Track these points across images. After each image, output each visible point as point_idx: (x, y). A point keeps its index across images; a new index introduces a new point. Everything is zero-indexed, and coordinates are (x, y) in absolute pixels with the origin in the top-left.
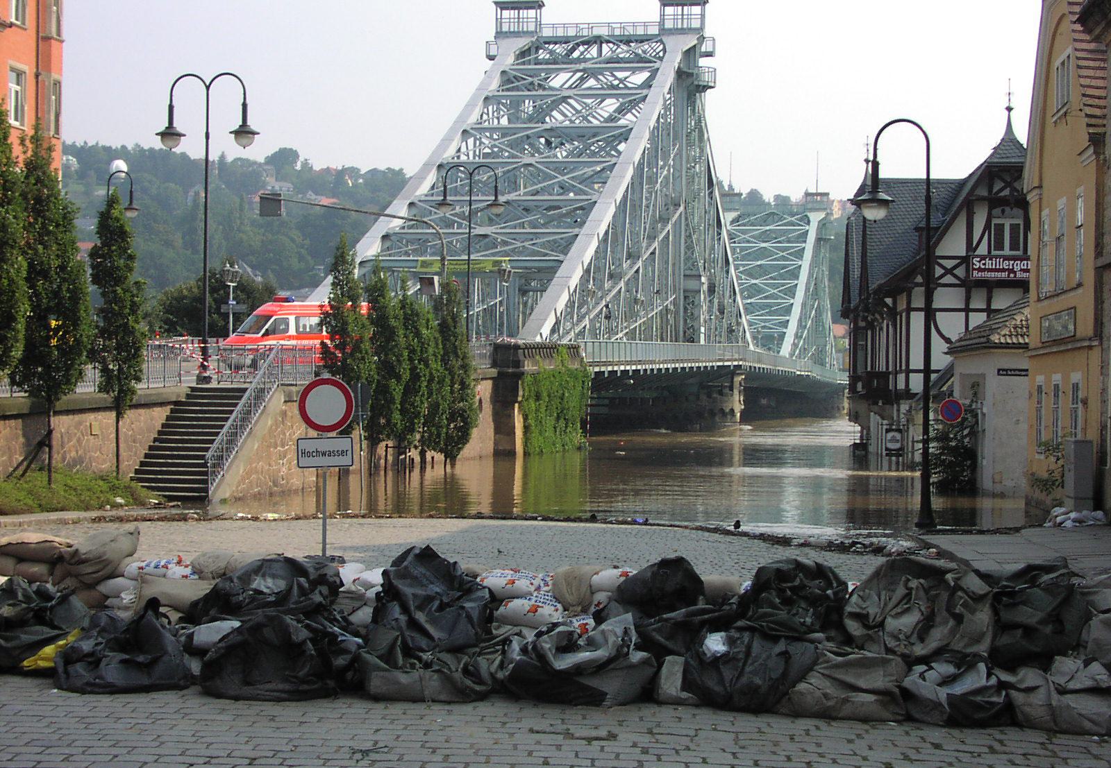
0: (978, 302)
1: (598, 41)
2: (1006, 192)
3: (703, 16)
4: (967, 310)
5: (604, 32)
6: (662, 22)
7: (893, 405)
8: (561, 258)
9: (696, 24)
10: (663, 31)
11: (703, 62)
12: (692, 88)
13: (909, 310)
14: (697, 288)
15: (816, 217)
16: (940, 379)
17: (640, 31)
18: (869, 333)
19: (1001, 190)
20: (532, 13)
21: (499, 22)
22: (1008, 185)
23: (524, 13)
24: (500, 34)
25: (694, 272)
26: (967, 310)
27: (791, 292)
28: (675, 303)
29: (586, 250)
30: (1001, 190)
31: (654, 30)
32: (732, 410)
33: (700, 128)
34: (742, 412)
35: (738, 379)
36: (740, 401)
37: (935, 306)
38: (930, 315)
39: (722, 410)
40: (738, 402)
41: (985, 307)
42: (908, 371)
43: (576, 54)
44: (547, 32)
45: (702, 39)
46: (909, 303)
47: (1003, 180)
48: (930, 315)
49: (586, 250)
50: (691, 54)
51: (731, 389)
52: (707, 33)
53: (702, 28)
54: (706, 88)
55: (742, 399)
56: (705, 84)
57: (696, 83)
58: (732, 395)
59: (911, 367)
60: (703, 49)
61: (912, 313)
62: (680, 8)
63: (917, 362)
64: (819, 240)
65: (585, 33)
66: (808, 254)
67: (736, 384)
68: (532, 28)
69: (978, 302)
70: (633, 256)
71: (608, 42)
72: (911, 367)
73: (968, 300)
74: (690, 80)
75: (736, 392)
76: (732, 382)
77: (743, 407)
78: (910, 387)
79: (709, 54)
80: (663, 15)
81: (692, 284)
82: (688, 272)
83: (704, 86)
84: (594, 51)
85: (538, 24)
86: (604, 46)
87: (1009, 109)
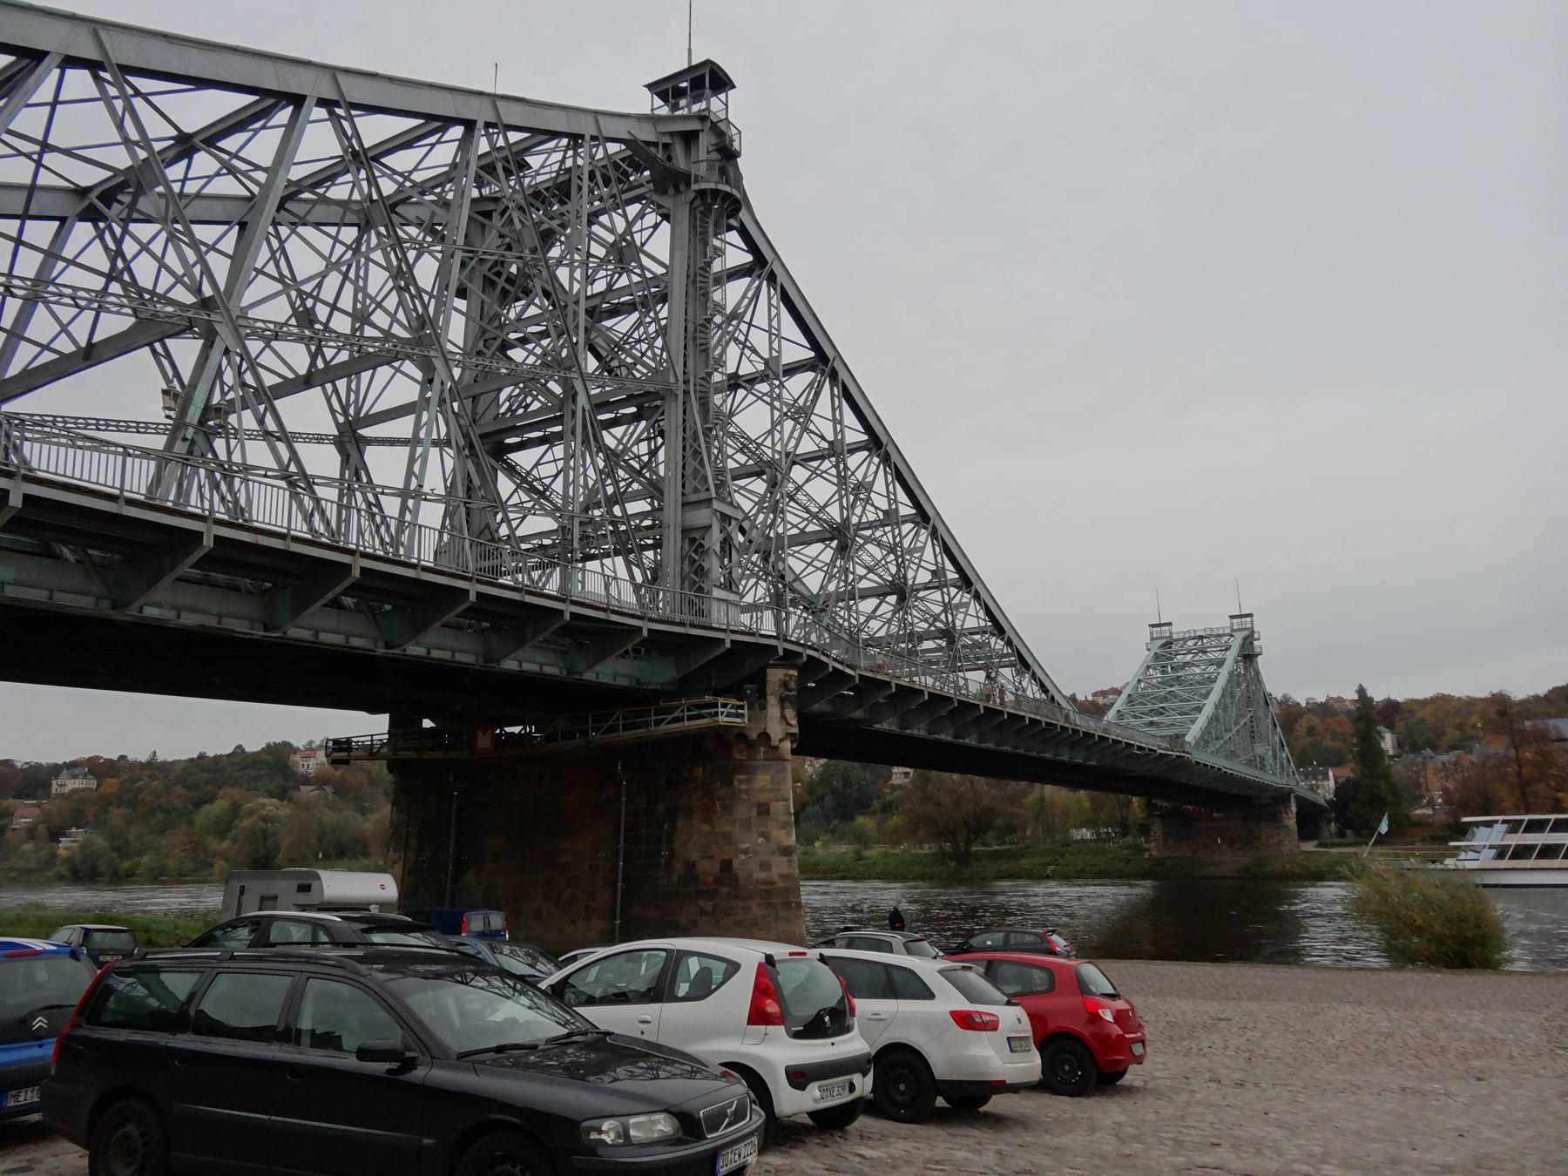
3: (1252, 622)
9: (1249, 626)
17: (1221, 632)
20: (1167, 628)
21: (1152, 633)
23: (1163, 628)
24: (1152, 639)
31: (1228, 631)
33: (1258, 673)
35: (1292, 795)
44: (1175, 637)
52: (1255, 629)
53: (1252, 628)
68: (1168, 635)
79: (1258, 639)
80: (1232, 624)
85: (1171, 633)
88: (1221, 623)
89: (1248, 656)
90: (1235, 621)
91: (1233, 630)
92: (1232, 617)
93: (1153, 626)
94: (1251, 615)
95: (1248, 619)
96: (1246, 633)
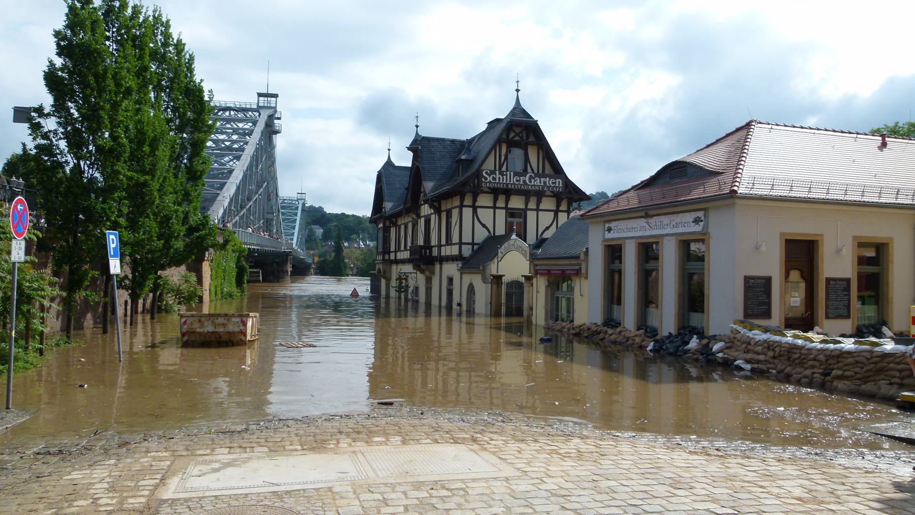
0: (501, 203)
1: (229, 109)
2: (517, 138)
3: (276, 101)
4: (495, 208)
5: (232, 106)
6: (258, 103)
7: (434, 264)
8: (218, 192)
11: (276, 121)
13: (461, 207)
15: (301, 202)
16: (479, 249)
17: (248, 106)
18: (393, 230)
19: (515, 136)
22: (517, 135)
25: (271, 211)
26: (495, 208)
27: (294, 228)
28: (263, 223)
29: (230, 189)
30: (515, 136)
31: (255, 107)
32: (287, 271)
34: (291, 272)
35: (290, 257)
37: (477, 204)
38: (475, 209)
41: (504, 206)
42: (461, 243)
43: (219, 114)
45: (276, 111)
46: (462, 201)
47: (515, 132)
48: (475, 209)
49: (230, 189)
50: (271, 118)
52: (278, 109)
53: (276, 107)
54: (278, 132)
59: (463, 241)
60: (276, 116)
61: (464, 209)
62: (266, 98)
63: (467, 238)
64: (302, 210)
65: (223, 105)
66: (299, 214)
67: (289, 259)
69: (501, 203)
70: (249, 200)
71: (234, 110)
72: (463, 241)
73: (495, 203)
74: (270, 128)
75: (289, 263)
76: (287, 259)
78: (463, 252)
79: (279, 118)
80: (258, 100)
81: (270, 216)
82: (268, 211)
84: (227, 114)
86: (232, 112)
87: (518, 91)
88: (250, 99)
89: (270, 131)
90: (261, 98)
91: (258, 106)
92: (298, 193)
94: (276, 96)
95: (273, 99)
96: (270, 112)
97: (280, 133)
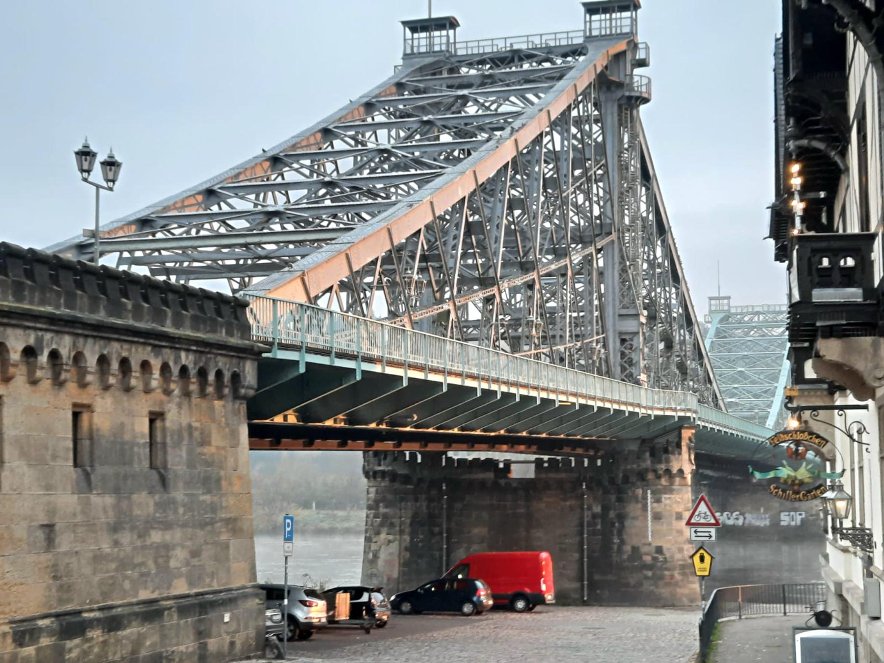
10: (589, 38)
11: (637, 71)
12: (623, 102)
14: (634, 330)
25: (631, 311)
32: (681, 471)
35: (687, 434)
36: (690, 460)
39: (668, 471)
40: (687, 461)
45: (634, 46)
51: (679, 446)
52: (640, 39)
55: (693, 457)
56: (638, 94)
57: (627, 94)
58: (680, 454)
60: (637, 57)
68: (444, 48)
75: (684, 449)
77: (694, 467)
79: (643, 63)
82: (624, 312)
83: (637, 98)
93: (415, 26)
97: (646, 100)
